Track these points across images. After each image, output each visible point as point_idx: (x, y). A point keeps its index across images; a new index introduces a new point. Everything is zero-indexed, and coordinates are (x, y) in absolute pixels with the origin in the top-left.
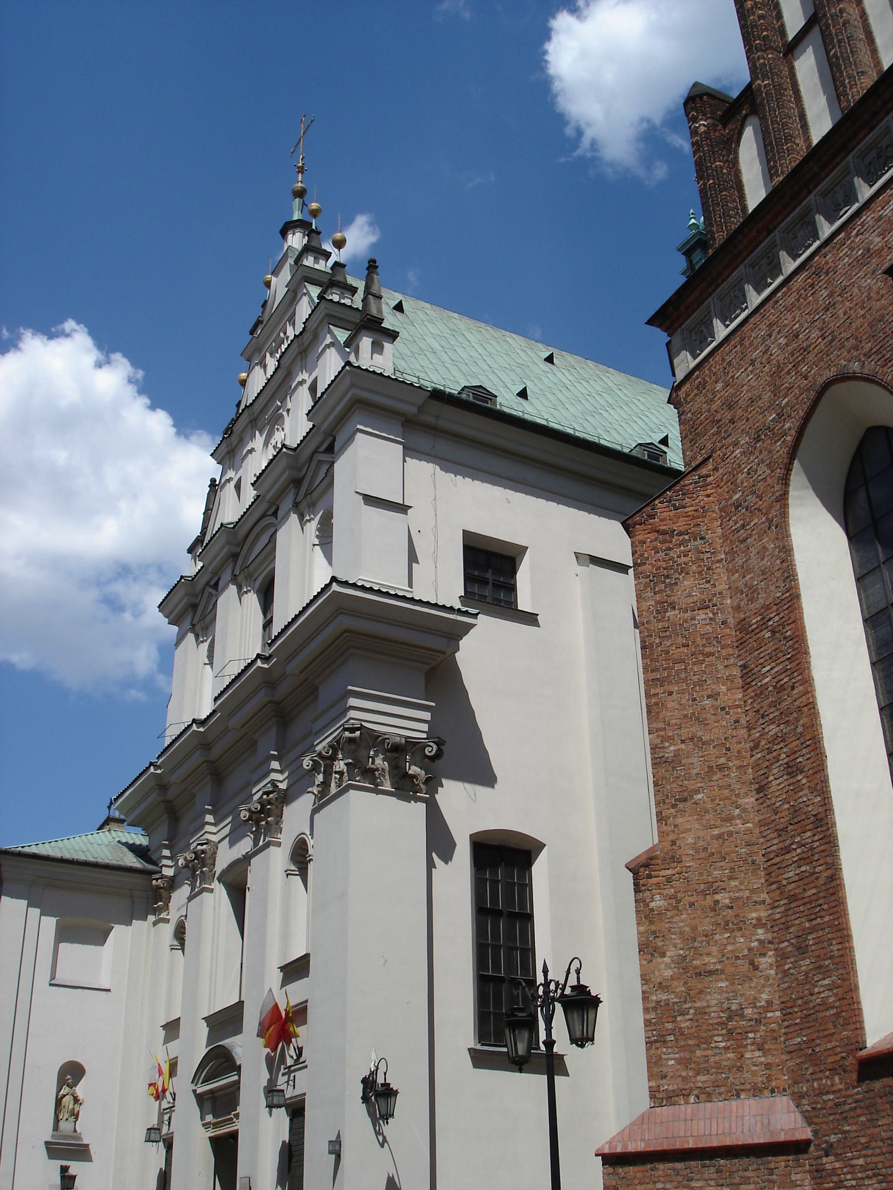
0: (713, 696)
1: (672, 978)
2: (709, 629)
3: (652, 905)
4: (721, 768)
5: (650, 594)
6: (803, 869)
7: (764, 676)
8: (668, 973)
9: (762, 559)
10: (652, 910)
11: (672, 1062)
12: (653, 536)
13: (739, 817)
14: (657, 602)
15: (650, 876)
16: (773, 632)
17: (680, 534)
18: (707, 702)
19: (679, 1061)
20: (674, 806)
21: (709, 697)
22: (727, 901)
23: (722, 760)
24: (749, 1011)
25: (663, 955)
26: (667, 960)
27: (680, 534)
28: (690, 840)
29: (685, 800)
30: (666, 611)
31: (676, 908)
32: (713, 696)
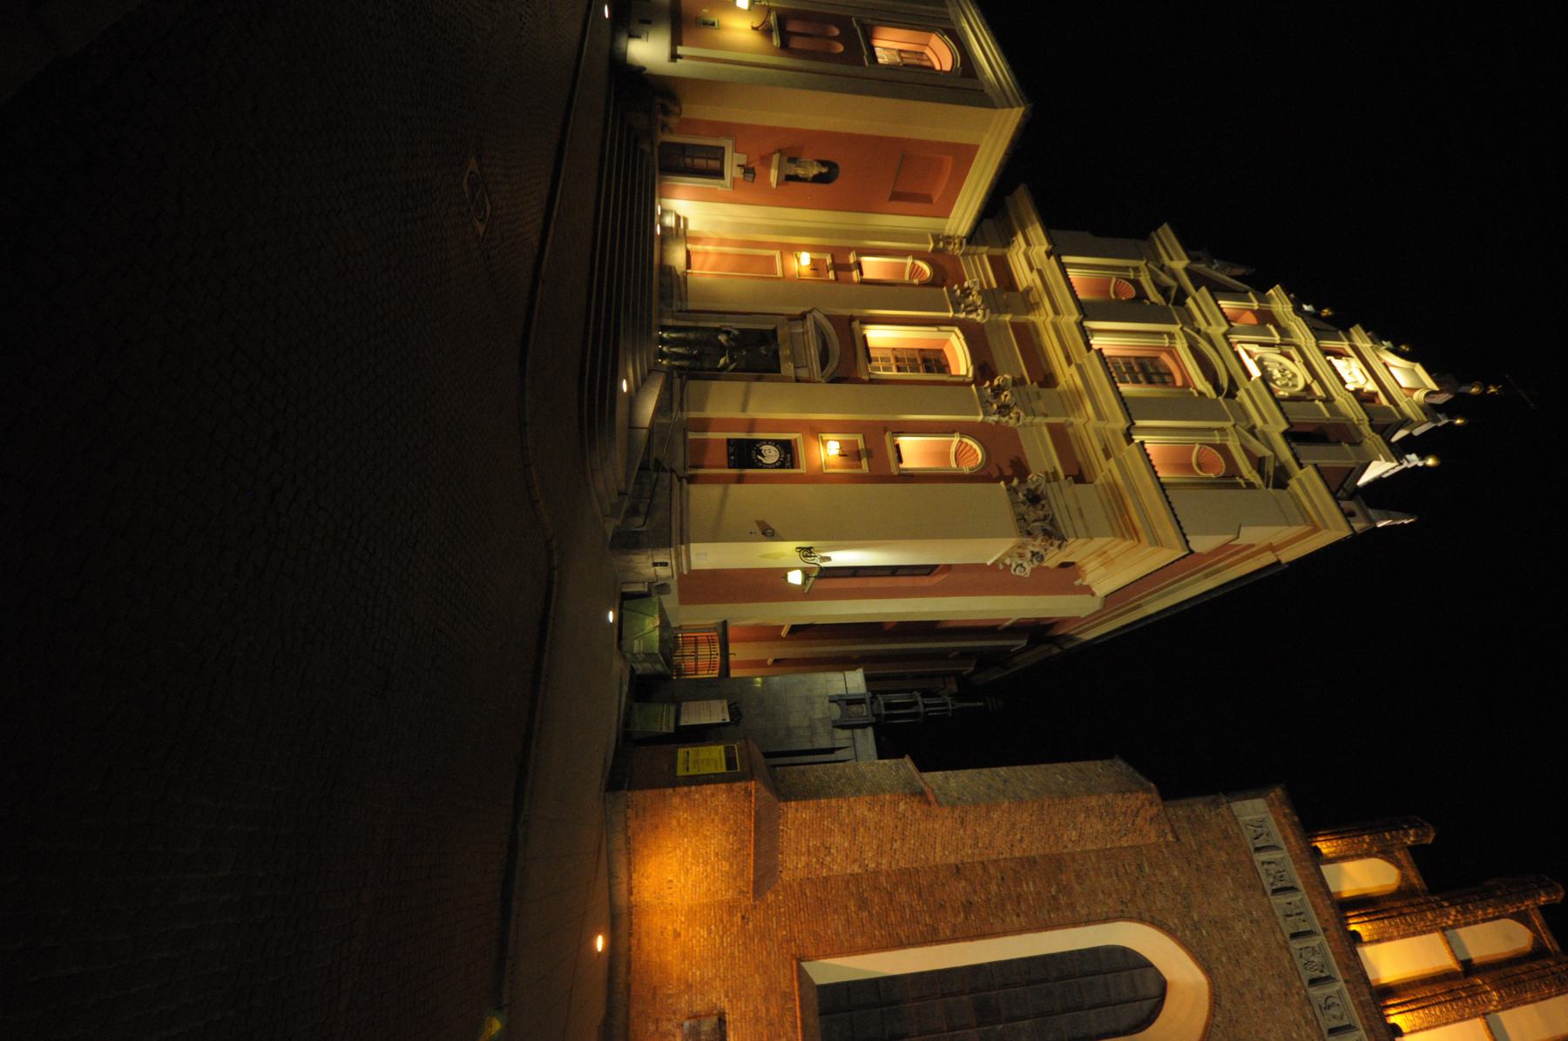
0: (1021, 840)
1: (855, 815)
2: (1065, 838)
3: (901, 804)
4: (976, 845)
5: (1100, 803)
6: (907, 911)
7: (1027, 884)
8: (858, 813)
9: (1103, 892)
10: (898, 803)
11: (804, 815)
12: (1139, 805)
13: (944, 854)
14: (1093, 807)
15: (920, 801)
16: (1054, 897)
17: (1134, 821)
18: (1018, 837)
19: (805, 818)
20: (959, 817)
21: (1022, 837)
22: (895, 846)
23: (980, 845)
24: (828, 859)
25: (869, 810)
26: (866, 813)
27: (1134, 821)
28: (937, 826)
29: (962, 823)
30: (1086, 813)
31: (897, 817)
32: (1021, 840)
